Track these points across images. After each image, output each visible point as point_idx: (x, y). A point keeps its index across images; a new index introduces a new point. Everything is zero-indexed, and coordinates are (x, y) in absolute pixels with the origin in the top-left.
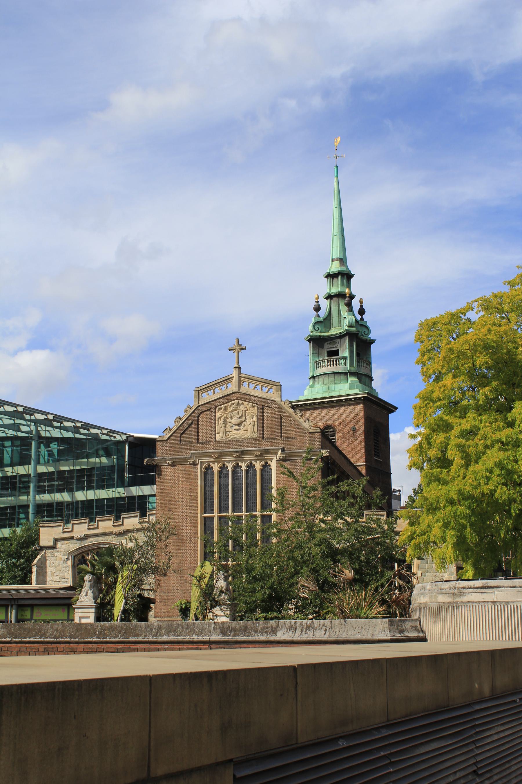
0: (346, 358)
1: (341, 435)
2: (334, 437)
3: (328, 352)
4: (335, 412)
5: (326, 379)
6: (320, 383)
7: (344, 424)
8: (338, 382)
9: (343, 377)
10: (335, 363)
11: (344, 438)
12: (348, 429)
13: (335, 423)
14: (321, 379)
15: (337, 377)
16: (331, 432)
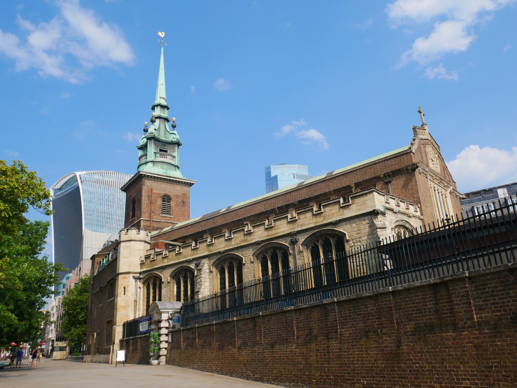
0: (174, 157)
1: (175, 203)
2: (169, 203)
3: (160, 149)
4: (171, 187)
5: (165, 166)
6: (159, 167)
7: (177, 196)
8: (171, 170)
9: (174, 168)
10: (166, 156)
11: (177, 205)
12: (180, 200)
13: (171, 195)
14: (160, 164)
15: (171, 166)
16: (167, 199)
